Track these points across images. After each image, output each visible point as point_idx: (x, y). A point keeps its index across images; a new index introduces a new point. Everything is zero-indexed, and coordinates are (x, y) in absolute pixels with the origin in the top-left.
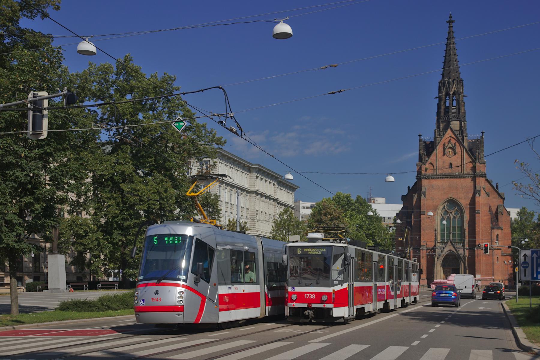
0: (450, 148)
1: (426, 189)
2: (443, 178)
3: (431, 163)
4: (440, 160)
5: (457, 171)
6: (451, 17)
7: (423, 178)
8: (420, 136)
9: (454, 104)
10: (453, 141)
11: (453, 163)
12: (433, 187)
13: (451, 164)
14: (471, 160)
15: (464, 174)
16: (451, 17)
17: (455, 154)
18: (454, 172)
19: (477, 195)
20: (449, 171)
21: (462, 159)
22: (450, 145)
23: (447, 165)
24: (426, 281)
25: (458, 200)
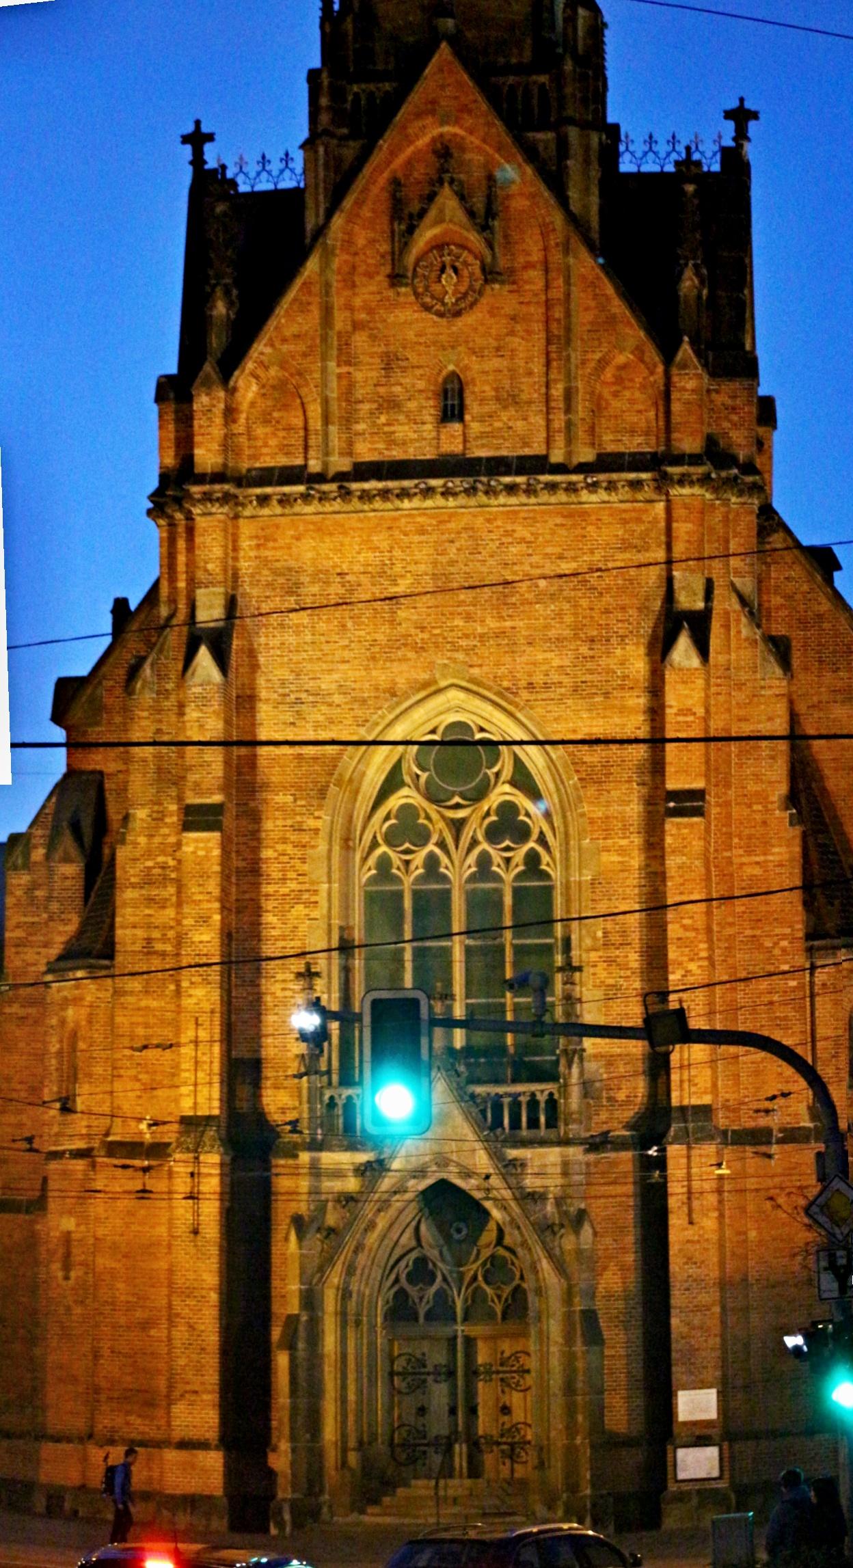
1: (231, 604)
4: (360, 340)
8: (197, 139)
19: (683, 651)
24: (214, 1461)
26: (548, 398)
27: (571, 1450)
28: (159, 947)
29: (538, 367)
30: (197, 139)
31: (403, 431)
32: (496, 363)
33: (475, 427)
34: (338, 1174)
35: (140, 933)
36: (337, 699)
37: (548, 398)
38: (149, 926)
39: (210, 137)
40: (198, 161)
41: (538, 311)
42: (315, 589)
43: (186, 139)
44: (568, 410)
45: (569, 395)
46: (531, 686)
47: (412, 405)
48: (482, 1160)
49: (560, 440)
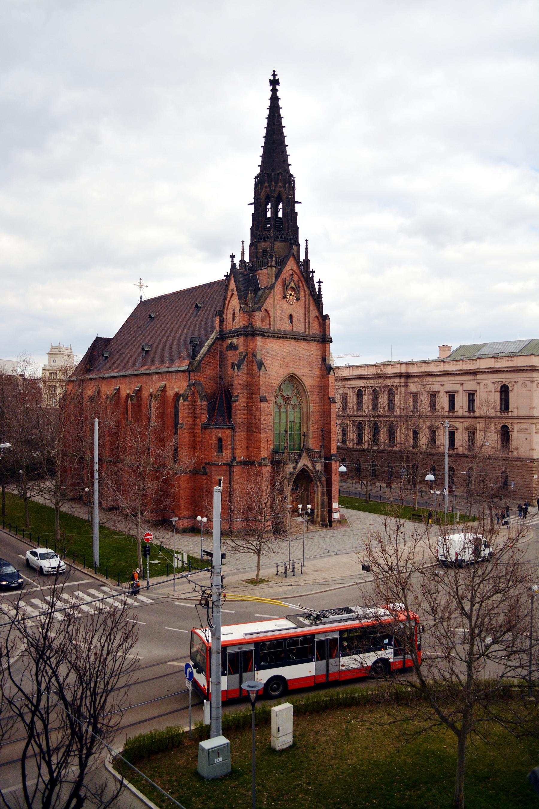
0: (292, 288)
2: (283, 338)
3: (266, 310)
5: (299, 328)
6: (274, 75)
7: (259, 335)
8: (233, 257)
9: (280, 215)
10: (296, 278)
11: (294, 315)
12: (268, 353)
13: (291, 316)
14: (317, 314)
15: (309, 336)
16: (274, 75)
17: (298, 299)
18: (295, 330)
20: (286, 326)
21: (307, 312)
22: (292, 285)
23: (286, 316)
25: (302, 377)
26: (305, 322)
27: (322, 515)
28: (244, 422)
29: (303, 316)
30: (233, 257)
31: (284, 325)
32: (298, 314)
33: (294, 326)
34: (289, 468)
35: (241, 420)
36: (275, 375)
37: (305, 322)
38: (242, 419)
39: (234, 256)
40: (232, 261)
41: (304, 305)
42: (272, 353)
43: (231, 256)
44: (309, 325)
45: (309, 322)
46: (303, 375)
47: (285, 320)
48: (310, 465)
49: (307, 330)
